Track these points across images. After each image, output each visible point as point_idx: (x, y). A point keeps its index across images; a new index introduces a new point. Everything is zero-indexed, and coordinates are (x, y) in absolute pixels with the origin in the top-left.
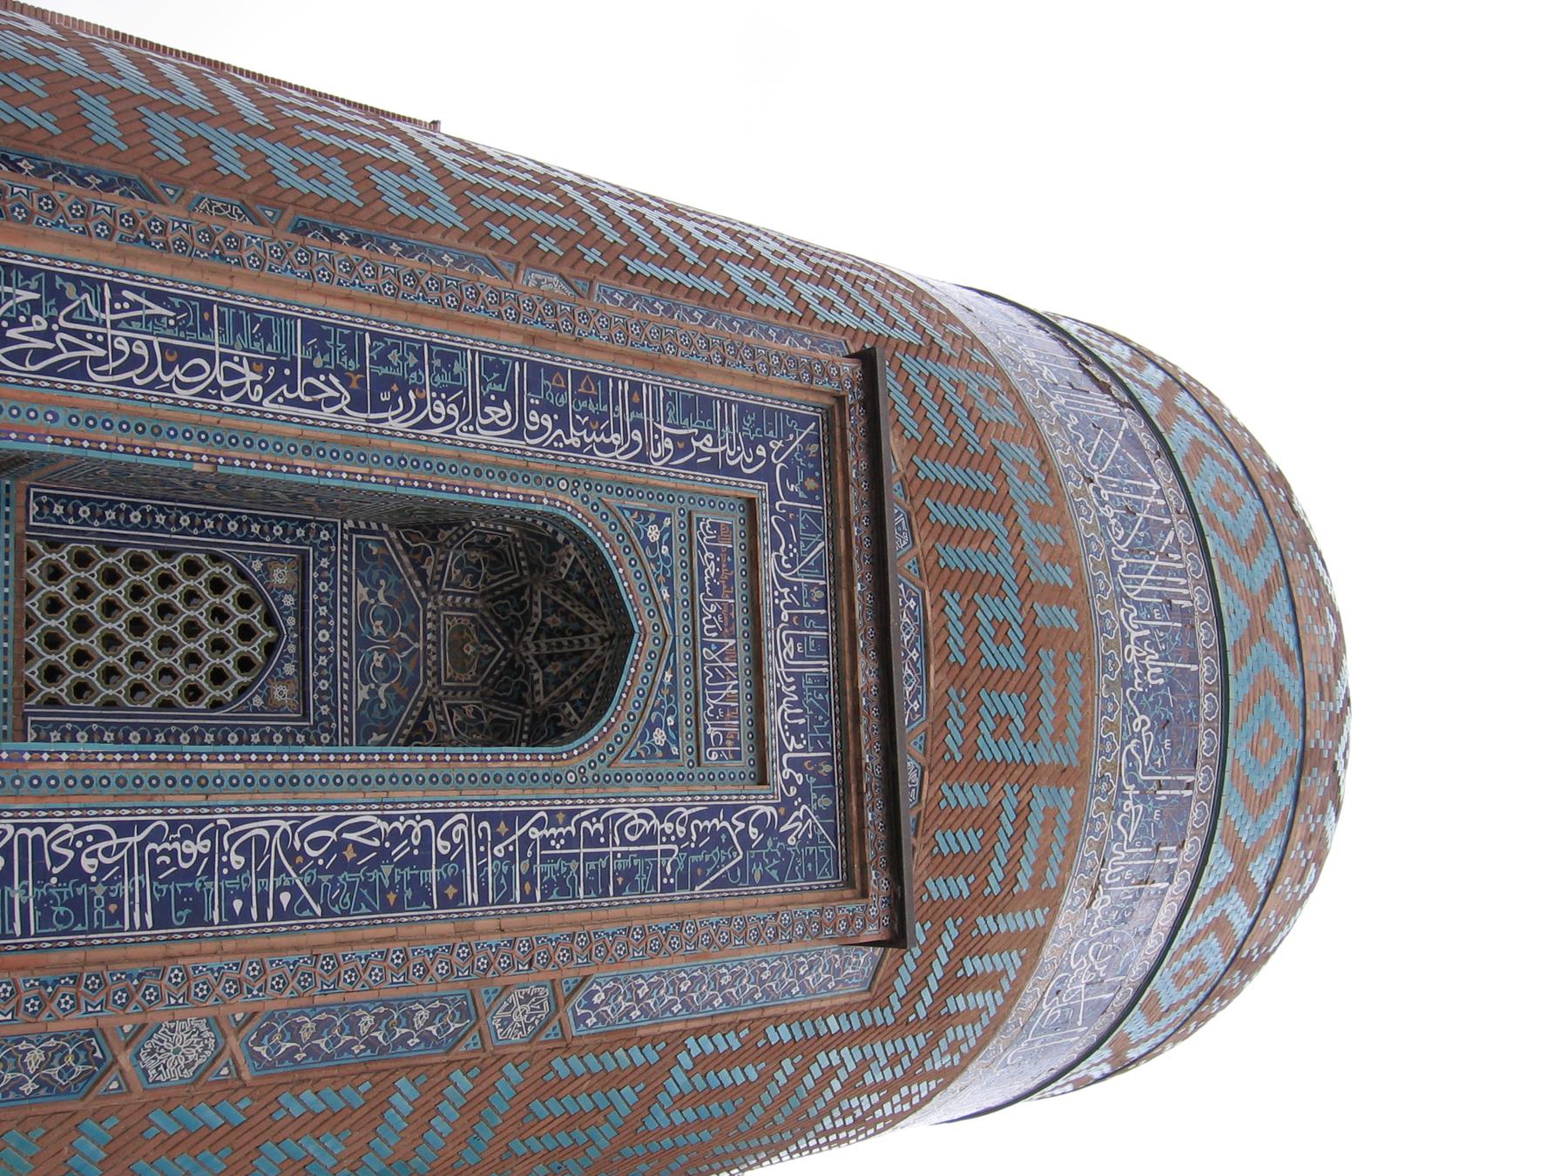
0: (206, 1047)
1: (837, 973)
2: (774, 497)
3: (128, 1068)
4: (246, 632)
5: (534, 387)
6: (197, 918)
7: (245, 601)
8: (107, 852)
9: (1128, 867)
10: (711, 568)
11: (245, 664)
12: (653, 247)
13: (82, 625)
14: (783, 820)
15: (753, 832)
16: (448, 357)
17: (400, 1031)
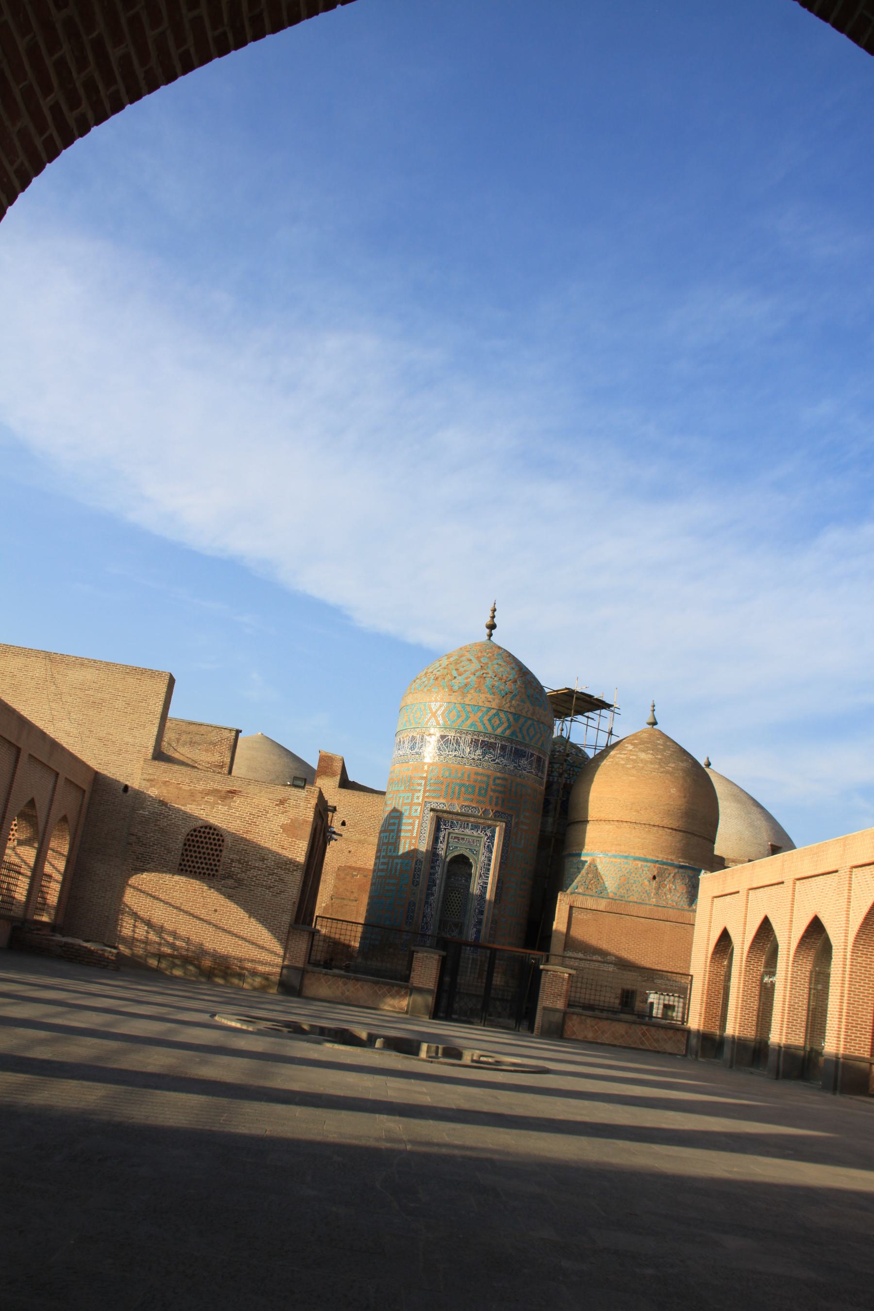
4: (455, 894)
5: (434, 863)
7: (452, 893)
10: (456, 840)
12: (410, 828)
13: (452, 911)
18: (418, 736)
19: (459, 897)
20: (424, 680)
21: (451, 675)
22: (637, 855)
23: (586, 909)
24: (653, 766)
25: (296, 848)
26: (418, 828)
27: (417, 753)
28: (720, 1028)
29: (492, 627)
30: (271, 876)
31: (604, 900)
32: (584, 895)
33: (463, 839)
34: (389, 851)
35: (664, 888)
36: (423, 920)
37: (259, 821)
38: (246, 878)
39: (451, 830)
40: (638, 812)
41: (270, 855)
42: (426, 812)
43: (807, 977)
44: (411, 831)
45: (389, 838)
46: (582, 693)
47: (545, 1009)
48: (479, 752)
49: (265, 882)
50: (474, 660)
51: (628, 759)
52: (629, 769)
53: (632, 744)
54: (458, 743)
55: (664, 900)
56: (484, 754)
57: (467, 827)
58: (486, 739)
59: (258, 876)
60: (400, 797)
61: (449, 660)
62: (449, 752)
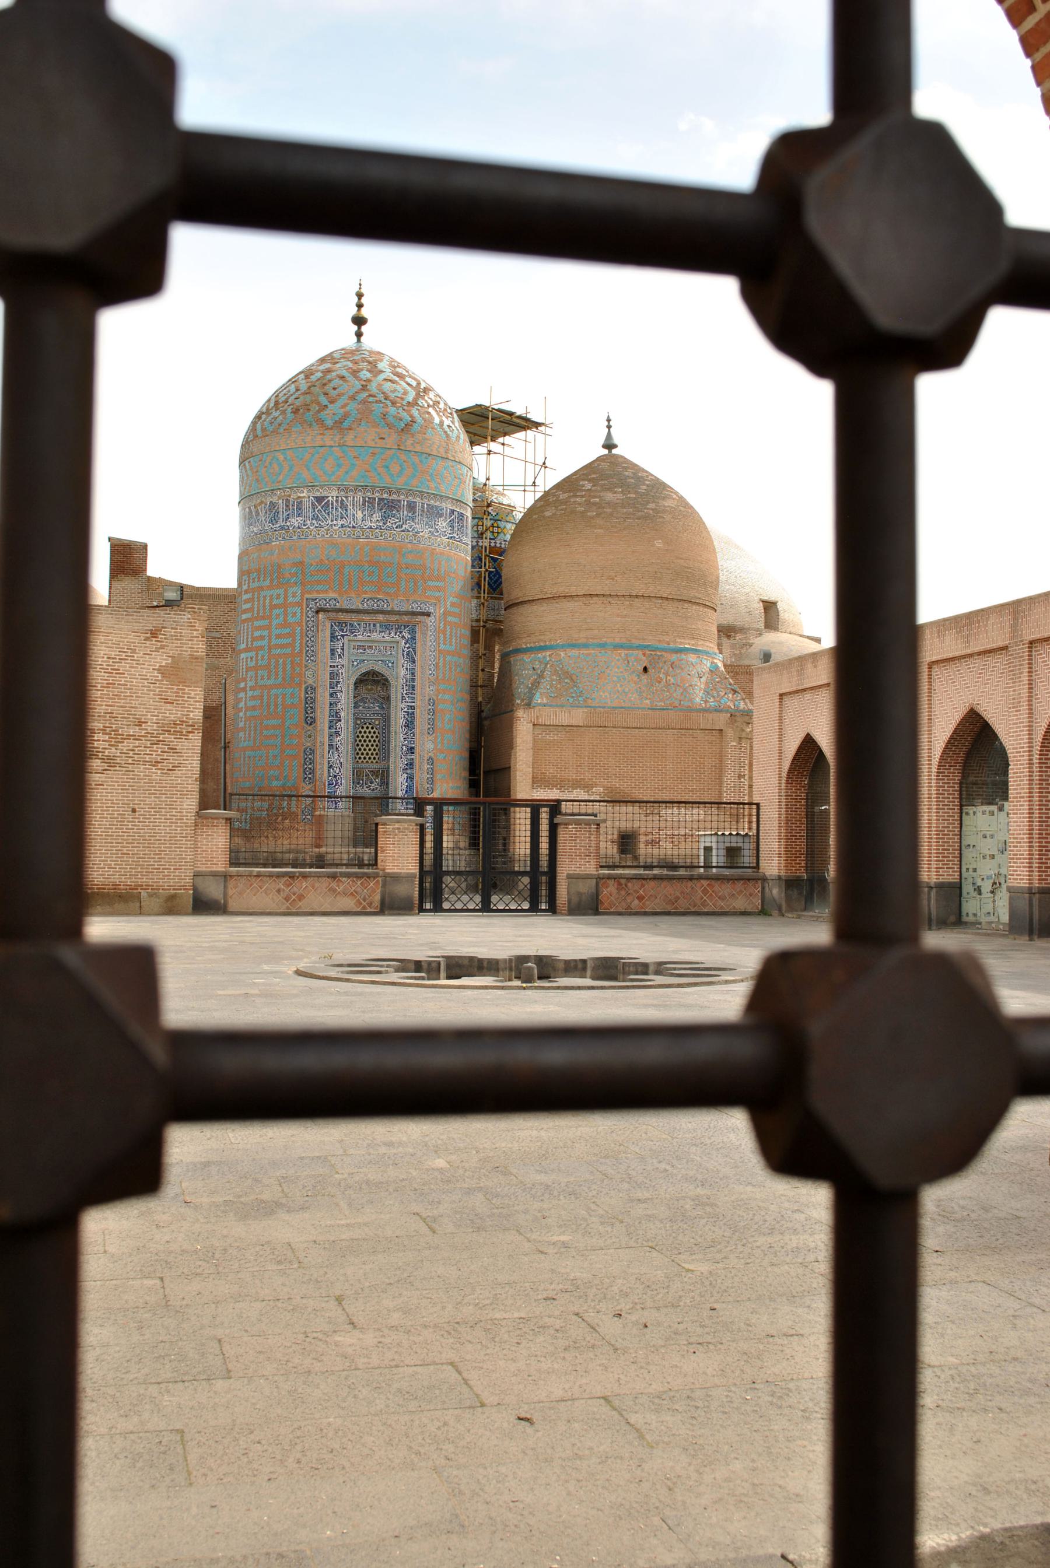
4: (367, 728)
6: (413, 748)
11: (372, 728)
13: (367, 754)
16: (331, 704)
18: (280, 501)
19: (374, 733)
20: (276, 414)
21: (318, 403)
22: (617, 640)
24: (625, 510)
25: (186, 699)
26: (301, 639)
27: (282, 528)
28: (807, 870)
29: (359, 321)
30: (155, 746)
31: (580, 710)
32: (550, 706)
33: (371, 647)
34: (259, 678)
35: (660, 682)
36: (329, 773)
37: (124, 666)
38: (118, 754)
39: (352, 637)
40: (613, 579)
41: (149, 714)
42: (310, 613)
43: (956, 791)
44: (292, 645)
45: (257, 660)
46: (499, 410)
47: (569, 877)
48: (377, 516)
49: (148, 756)
50: (350, 378)
51: (588, 503)
52: (592, 518)
53: (589, 481)
54: (344, 506)
55: (661, 701)
56: (385, 519)
57: (375, 630)
58: (385, 496)
59: (136, 749)
60: (265, 597)
61: (309, 380)
62: (332, 521)
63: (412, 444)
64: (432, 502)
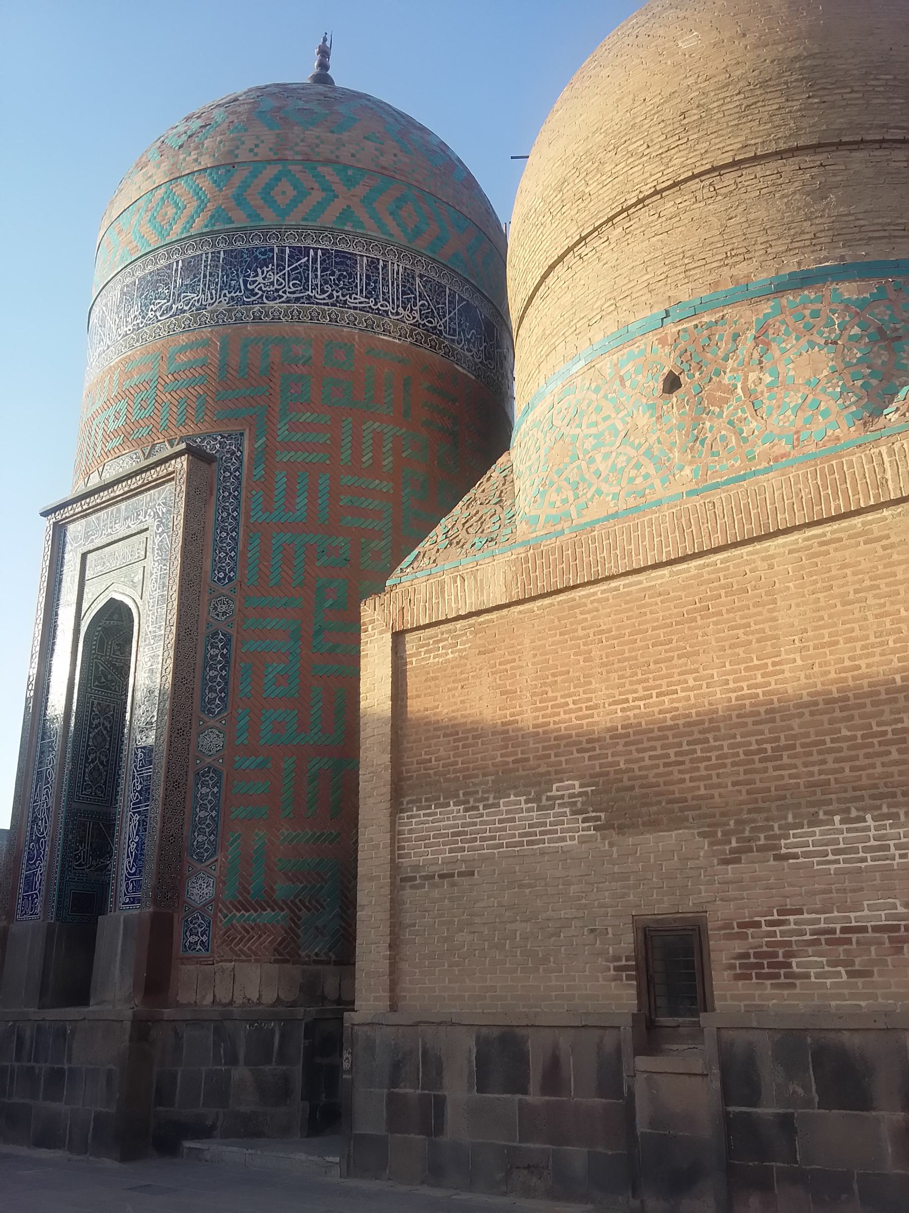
0: (211, 732)
1: (233, 453)
2: (80, 546)
3: (213, 758)
8: (137, 782)
9: (209, 289)
14: (159, 517)
15: (160, 529)
17: (219, 658)
23: (447, 621)
63: (196, 160)
64: (239, 245)
